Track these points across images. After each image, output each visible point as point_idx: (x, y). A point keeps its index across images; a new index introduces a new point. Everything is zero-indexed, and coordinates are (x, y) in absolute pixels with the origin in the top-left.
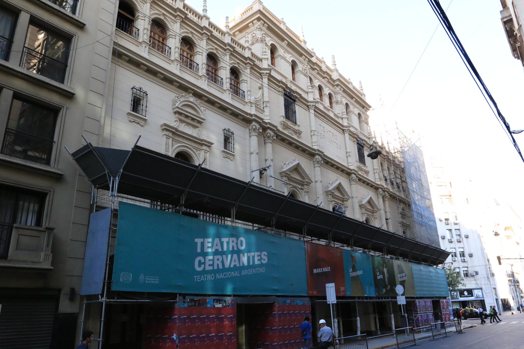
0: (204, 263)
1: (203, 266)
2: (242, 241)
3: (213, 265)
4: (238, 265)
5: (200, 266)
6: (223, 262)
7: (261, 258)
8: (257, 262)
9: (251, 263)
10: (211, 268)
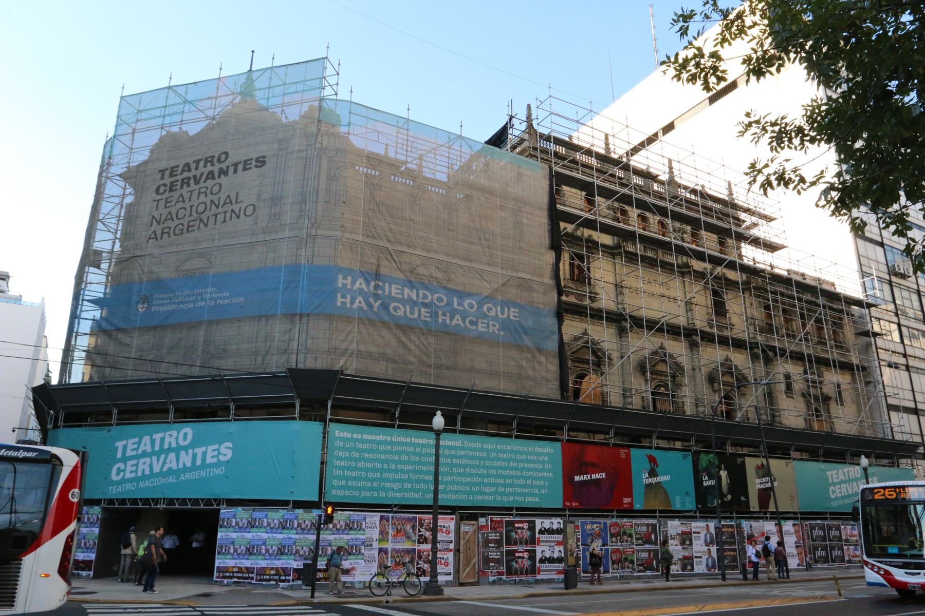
0: (124, 471)
1: (122, 474)
2: (186, 435)
3: (136, 471)
4: (175, 467)
5: (118, 474)
6: (151, 466)
7: (219, 453)
8: (209, 460)
9: (199, 462)
10: (133, 475)
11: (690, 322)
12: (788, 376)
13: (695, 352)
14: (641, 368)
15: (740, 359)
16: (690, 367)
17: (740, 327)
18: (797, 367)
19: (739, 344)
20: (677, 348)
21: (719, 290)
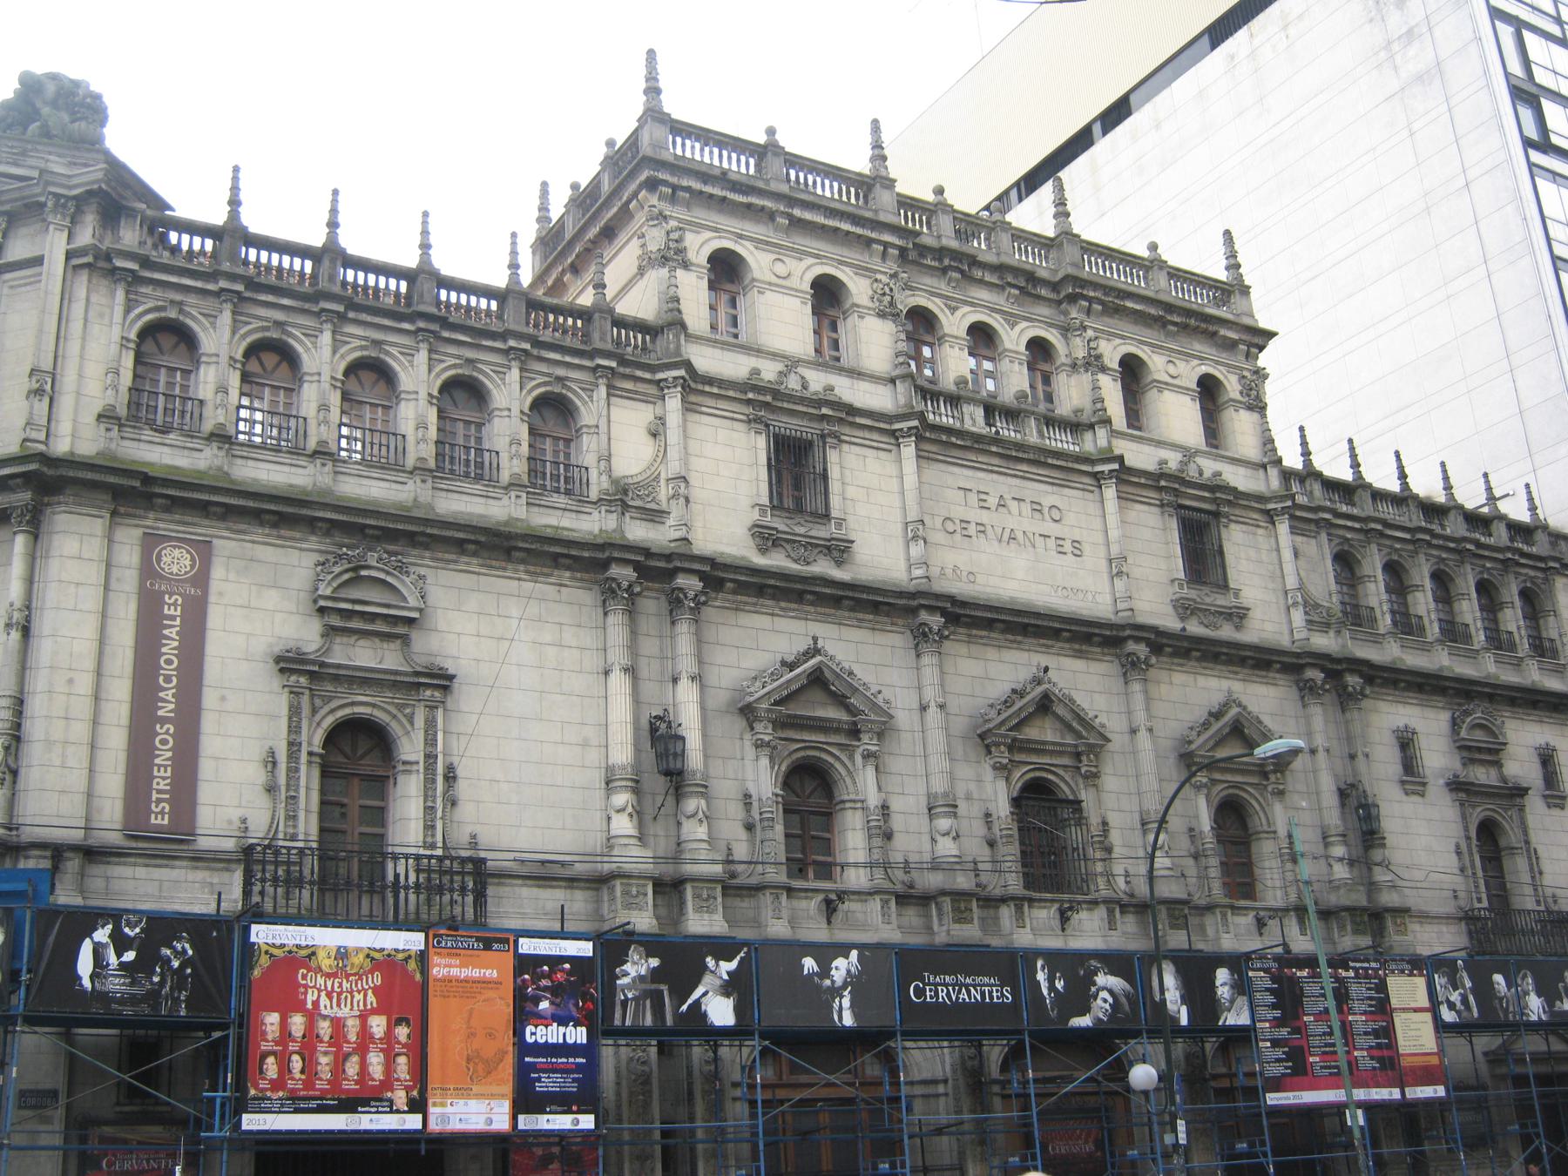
11: (1121, 606)
12: (1406, 743)
13: (1136, 687)
14: (985, 740)
15: (1264, 699)
16: (1125, 727)
17: (1270, 620)
18: (1430, 713)
19: (1260, 660)
20: (1085, 682)
21: (1201, 520)
